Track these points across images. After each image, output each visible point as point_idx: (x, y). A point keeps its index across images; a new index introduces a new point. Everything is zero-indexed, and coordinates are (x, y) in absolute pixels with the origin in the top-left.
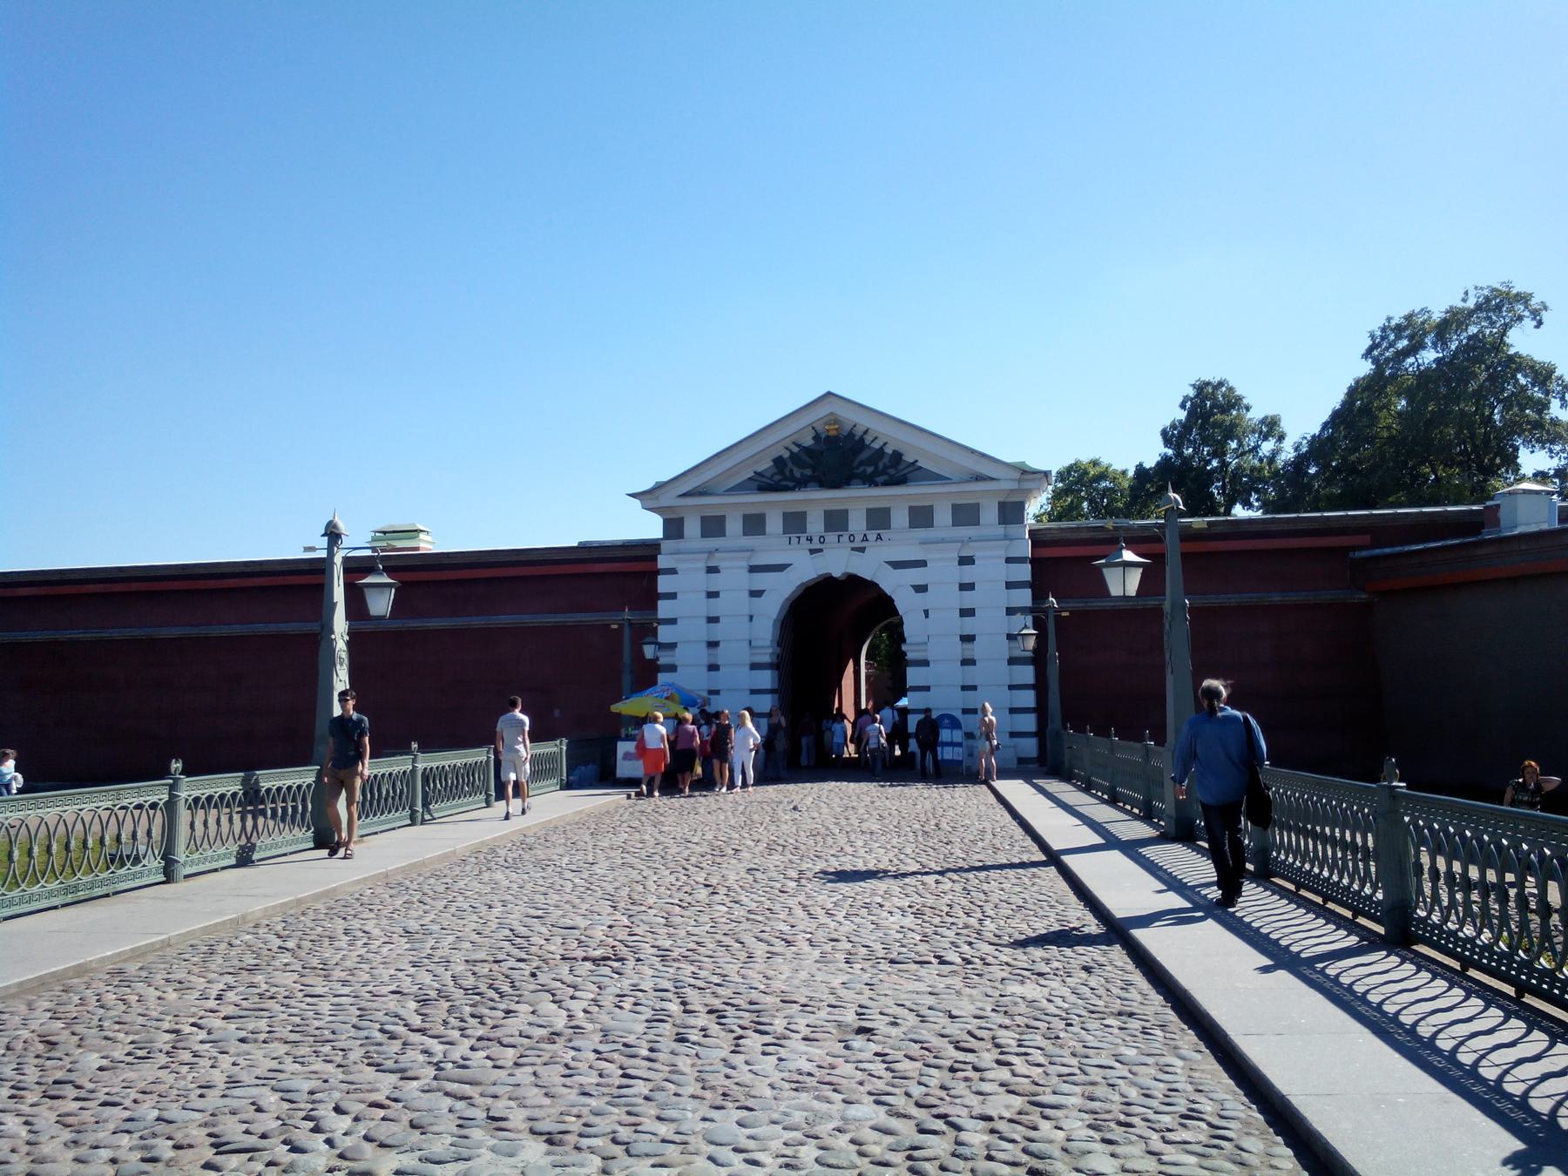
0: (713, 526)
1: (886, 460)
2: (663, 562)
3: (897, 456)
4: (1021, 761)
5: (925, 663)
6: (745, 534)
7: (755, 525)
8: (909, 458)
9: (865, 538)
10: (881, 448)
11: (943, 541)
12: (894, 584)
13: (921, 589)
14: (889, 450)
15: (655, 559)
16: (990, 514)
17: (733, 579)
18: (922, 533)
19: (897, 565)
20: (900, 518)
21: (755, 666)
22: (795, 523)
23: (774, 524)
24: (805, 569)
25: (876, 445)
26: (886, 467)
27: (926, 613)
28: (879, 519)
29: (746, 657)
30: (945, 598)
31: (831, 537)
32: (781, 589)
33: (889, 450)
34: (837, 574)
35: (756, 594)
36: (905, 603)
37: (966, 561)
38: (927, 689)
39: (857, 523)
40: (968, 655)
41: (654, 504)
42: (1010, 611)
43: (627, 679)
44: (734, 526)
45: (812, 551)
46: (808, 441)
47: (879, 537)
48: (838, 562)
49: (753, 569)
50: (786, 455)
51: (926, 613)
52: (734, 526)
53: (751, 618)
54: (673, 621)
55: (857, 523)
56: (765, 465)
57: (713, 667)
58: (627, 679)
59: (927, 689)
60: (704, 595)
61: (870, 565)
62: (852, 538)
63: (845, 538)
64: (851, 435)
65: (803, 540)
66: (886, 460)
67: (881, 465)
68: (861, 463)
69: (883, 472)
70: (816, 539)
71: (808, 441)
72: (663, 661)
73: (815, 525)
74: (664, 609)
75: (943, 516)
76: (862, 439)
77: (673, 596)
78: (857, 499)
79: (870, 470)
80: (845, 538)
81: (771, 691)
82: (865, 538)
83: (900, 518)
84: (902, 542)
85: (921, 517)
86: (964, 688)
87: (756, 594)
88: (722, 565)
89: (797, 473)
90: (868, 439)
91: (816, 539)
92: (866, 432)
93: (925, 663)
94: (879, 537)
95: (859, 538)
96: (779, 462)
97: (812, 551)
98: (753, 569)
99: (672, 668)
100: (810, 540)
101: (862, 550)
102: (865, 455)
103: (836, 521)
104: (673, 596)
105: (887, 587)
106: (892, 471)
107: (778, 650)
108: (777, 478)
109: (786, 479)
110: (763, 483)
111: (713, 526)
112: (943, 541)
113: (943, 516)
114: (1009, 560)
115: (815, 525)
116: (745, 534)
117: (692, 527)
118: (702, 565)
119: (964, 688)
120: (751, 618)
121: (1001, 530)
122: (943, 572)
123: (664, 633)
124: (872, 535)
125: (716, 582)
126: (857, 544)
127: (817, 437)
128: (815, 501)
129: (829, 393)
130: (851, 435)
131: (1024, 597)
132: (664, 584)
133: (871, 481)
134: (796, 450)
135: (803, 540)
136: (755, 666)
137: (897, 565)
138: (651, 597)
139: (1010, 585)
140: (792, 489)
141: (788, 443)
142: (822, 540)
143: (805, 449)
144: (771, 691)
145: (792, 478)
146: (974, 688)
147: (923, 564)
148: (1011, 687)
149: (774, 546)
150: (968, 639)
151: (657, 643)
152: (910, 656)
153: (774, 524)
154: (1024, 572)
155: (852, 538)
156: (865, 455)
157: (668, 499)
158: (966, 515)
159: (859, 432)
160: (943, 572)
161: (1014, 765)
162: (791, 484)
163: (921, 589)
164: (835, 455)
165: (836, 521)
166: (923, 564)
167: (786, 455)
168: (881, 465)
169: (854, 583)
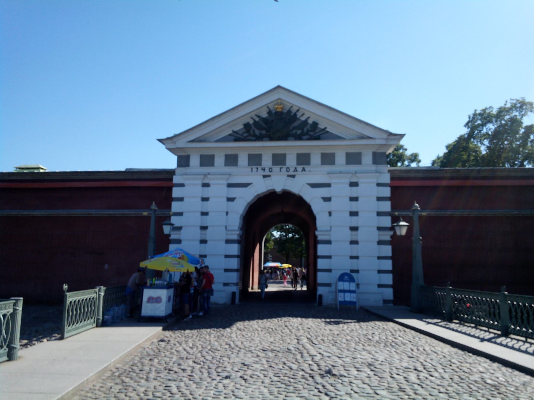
0: (207, 160)
1: (308, 127)
2: (176, 180)
3: (315, 124)
4: (385, 301)
5: (329, 242)
6: (226, 165)
7: (231, 160)
8: (321, 126)
9: (296, 170)
10: (306, 121)
11: (341, 172)
13: (327, 199)
14: (310, 121)
15: (171, 180)
17: (218, 191)
19: (314, 186)
20: (316, 159)
21: (228, 241)
23: (243, 160)
24: (260, 186)
25: (303, 119)
26: (308, 131)
27: (330, 214)
28: (304, 160)
29: (224, 236)
30: (341, 205)
31: (276, 169)
33: (310, 121)
34: (278, 189)
35: (230, 200)
37: (354, 184)
38: (329, 257)
39: (291, 161)
40: (354, 238)
41: (172, 146)
42: (379, 214)
43: (151, 246)
44: (219, 160)
45: (264, 176)
46: (265, 115)
47: (304, 170)
48: (279, 183)
49: (230, 185)
50: (251, 122)
51: (330, 214)
52: (219, 160)
53: (227, 213)
54: (180, 214)
55: (291, 161)
56: (239, 127)
57: (203, 241)
58: (151, 246)
59: (329, 257)
60: (200, 199)
62: (288, 169)
63: (284, 169)
64: (289, 111)
65: (260, 169)
66: (308, 127)
67: (305, 130)
68: (294, 128)
69: (307, 133)
70: (267, 170)
71: (265, 115)
72: (173, 237)
73: (267, 161)
74: (175, 207)
75: (340, 159)
76: (295, 115)
77: (181, 199)
78: (291, 148)
79: (299, 132)
80: (284, 169)
81: (237, 256)
82: (296, 170)
83: (316, 159)
84: (317, 173)
85: (328, 159)
86: (352, 257)
87: (230, 200)
88: (211, 182)
89: (257, 132)
90: (299, 114)
91: (267, 170)
92: (298, 111)
93: (329, 242)
94: (304, 170)
95: (292, 169)
96: (247, 126)
97: (264, 176)
98: (230, 185)
99: (179, 241)
100: (264, 170)
101: (293, 176)
102: (296, 124)
103: (279, 160)
104: (181, 199)
105: (307, 198)
106: (312, 133)
107: (241, 232)
108: (245, 135)
109: (250, 135)
110: (236, 137)
111: (207, 160)
112: (341, 172)
113: (340, 159)
114: (379, 185)
115: (267, 161)
116: (226, 165)
117: (195, 161)
118: (200, 182)
119: (352, 257)
120: (227, 213)
121: (374, 168)
122: (340, 190)
123: (175, 220)
124: (300, 168)
126: (291, 173)
127: (270, 113)
128: (268, 148)
129: (279, 87)
130: (289, 111)
132: (176, 192)
133: (299, 138)
134: (257, 119)
135: (260, 169)
136: (228, 241)
137: (314, 186)
139: (379, 199)
140: (255, 140)
141: (253, 115)
142: (271, 170)
143: (264, 120)
144: (237, 256)
145: (255, 135)
146: (357, 258)
147: (328, 185)
148: (379, 258)
149: (242, 173)
150: (354, 229)
151: (172, 225)
152: (320, 238)
153: (243, 160)
154: (387, 192)
155: (288, 169)
156: (296, 124)
157: (181, 143)
159: (294, 110)
161: (381, 304)
162: (253, 138)
163: (327, 199)
164: (280, 123)
165: (279, 160)
166: (328, 185)
167: (251, 122)
168: (305, 130)
169: (287, 195)
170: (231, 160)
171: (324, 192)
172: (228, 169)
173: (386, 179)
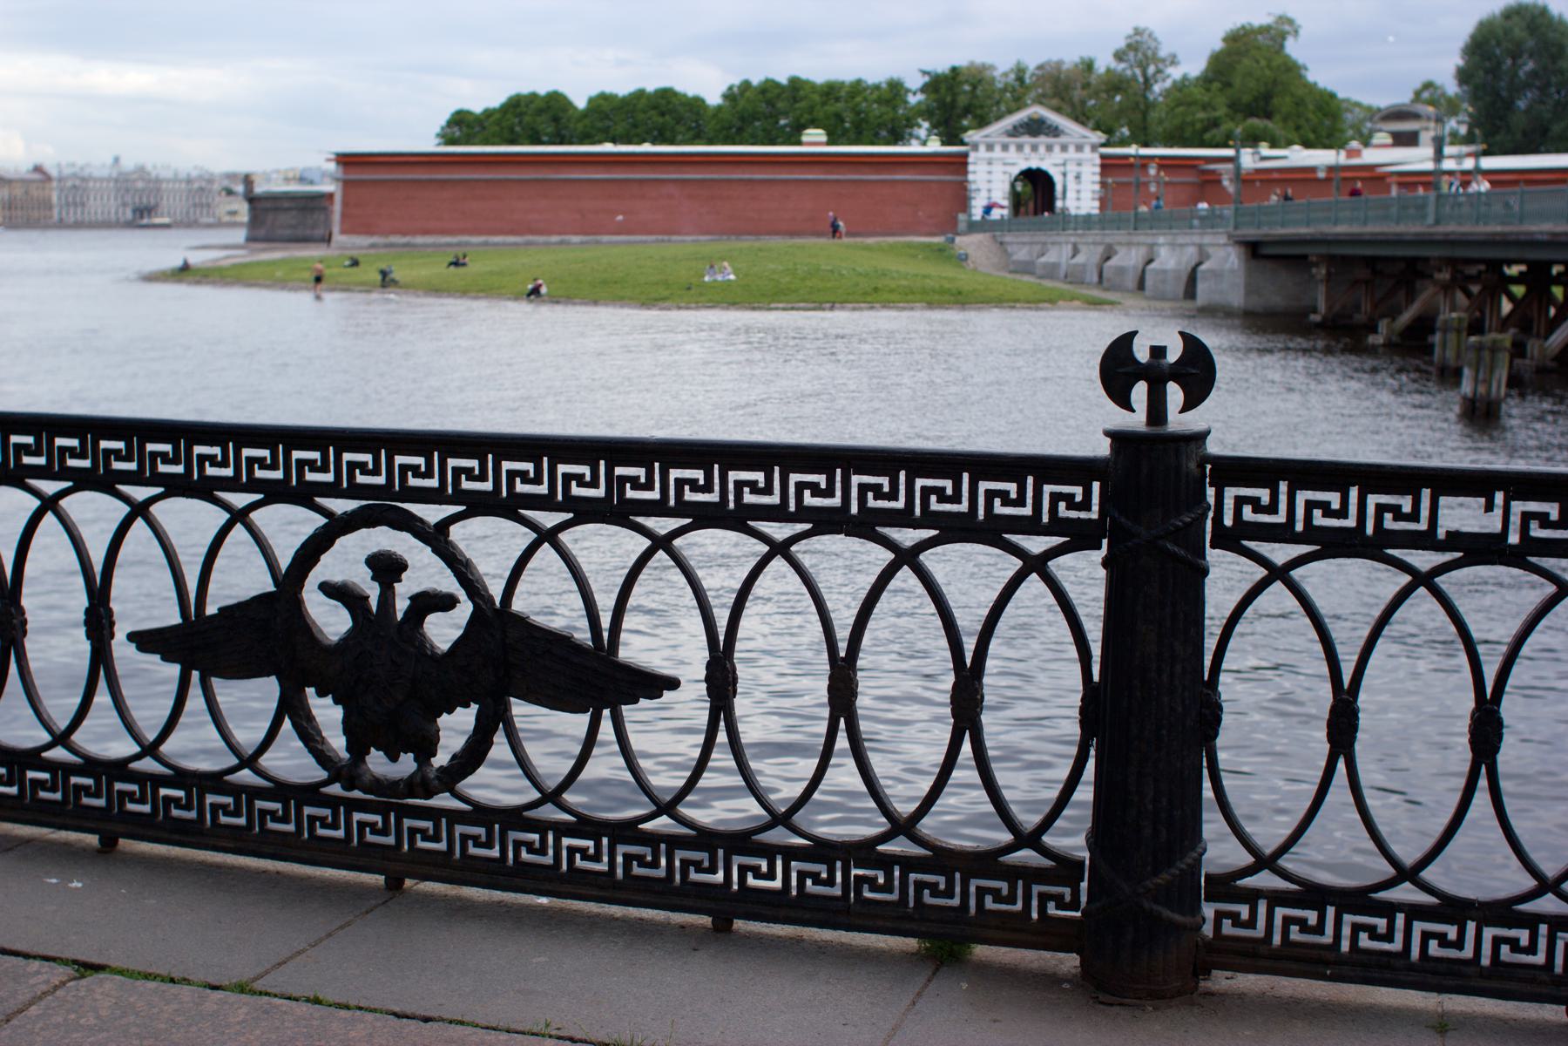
0: (990, 147)
2: (970, 160)
7: (1005, 148)
18: (1065, 156)
22: (1020, 148)
24: (1024, 166)
28: (1049, 148)
48: (1034, 164)
61: (1045, 166)
84: (1058, 156)
85: (1064, 148)
96: (1015, 128)
111: (990, 147)
131: (1098, 178)
132: (971, 168)
138: (966, 173)
154: (1098, 170)
158: (1079, 148)
170: (1005, 148)
172: (1004, 155)
173: (1098, 161)
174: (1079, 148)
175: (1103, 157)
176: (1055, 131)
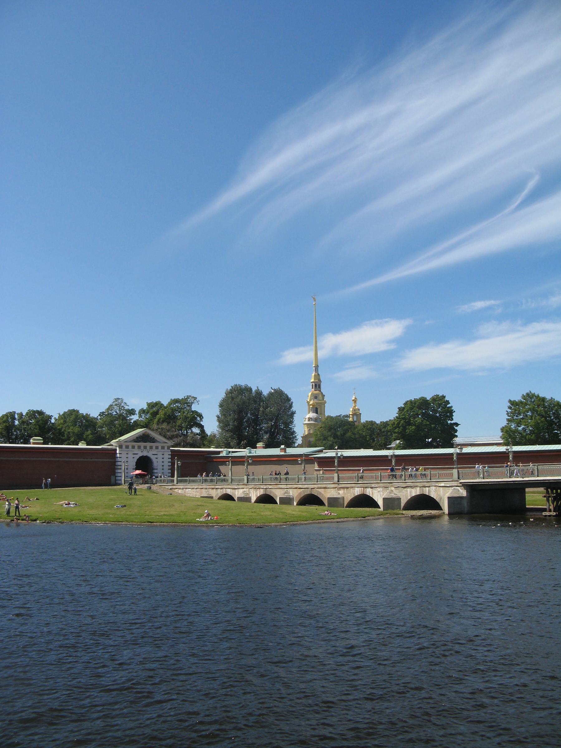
0: (127, 447)
7: (133, 447)
12: (153, 458)
16: (166, 448)
20: (154, 448)
22: (139, 447)
23: (136, 447)
24: (141, 454)
28: (151, 448)
32: (137, 457)
36: (154, 460)
39: (148, 448)
48: (145, 454)
55: (148, 448)
61: (150, 455)
73: (142, 448)
75: (160, 448)
78: (148, 444)
83: (154, 448)
85: (157, 448)
103: (145, 447)
113: (160, 448)
115: (142, 448)
125: (127, 456)
128: (142, 444)
149: (136, 451)
153: (136, 447)
154: (170, 457)
160: (160, 456)
165: (145, 447)
171: (156, 456)
173: (170, 453)
174: (163, 448)
175: (172, 451)
176: (153, 440)
